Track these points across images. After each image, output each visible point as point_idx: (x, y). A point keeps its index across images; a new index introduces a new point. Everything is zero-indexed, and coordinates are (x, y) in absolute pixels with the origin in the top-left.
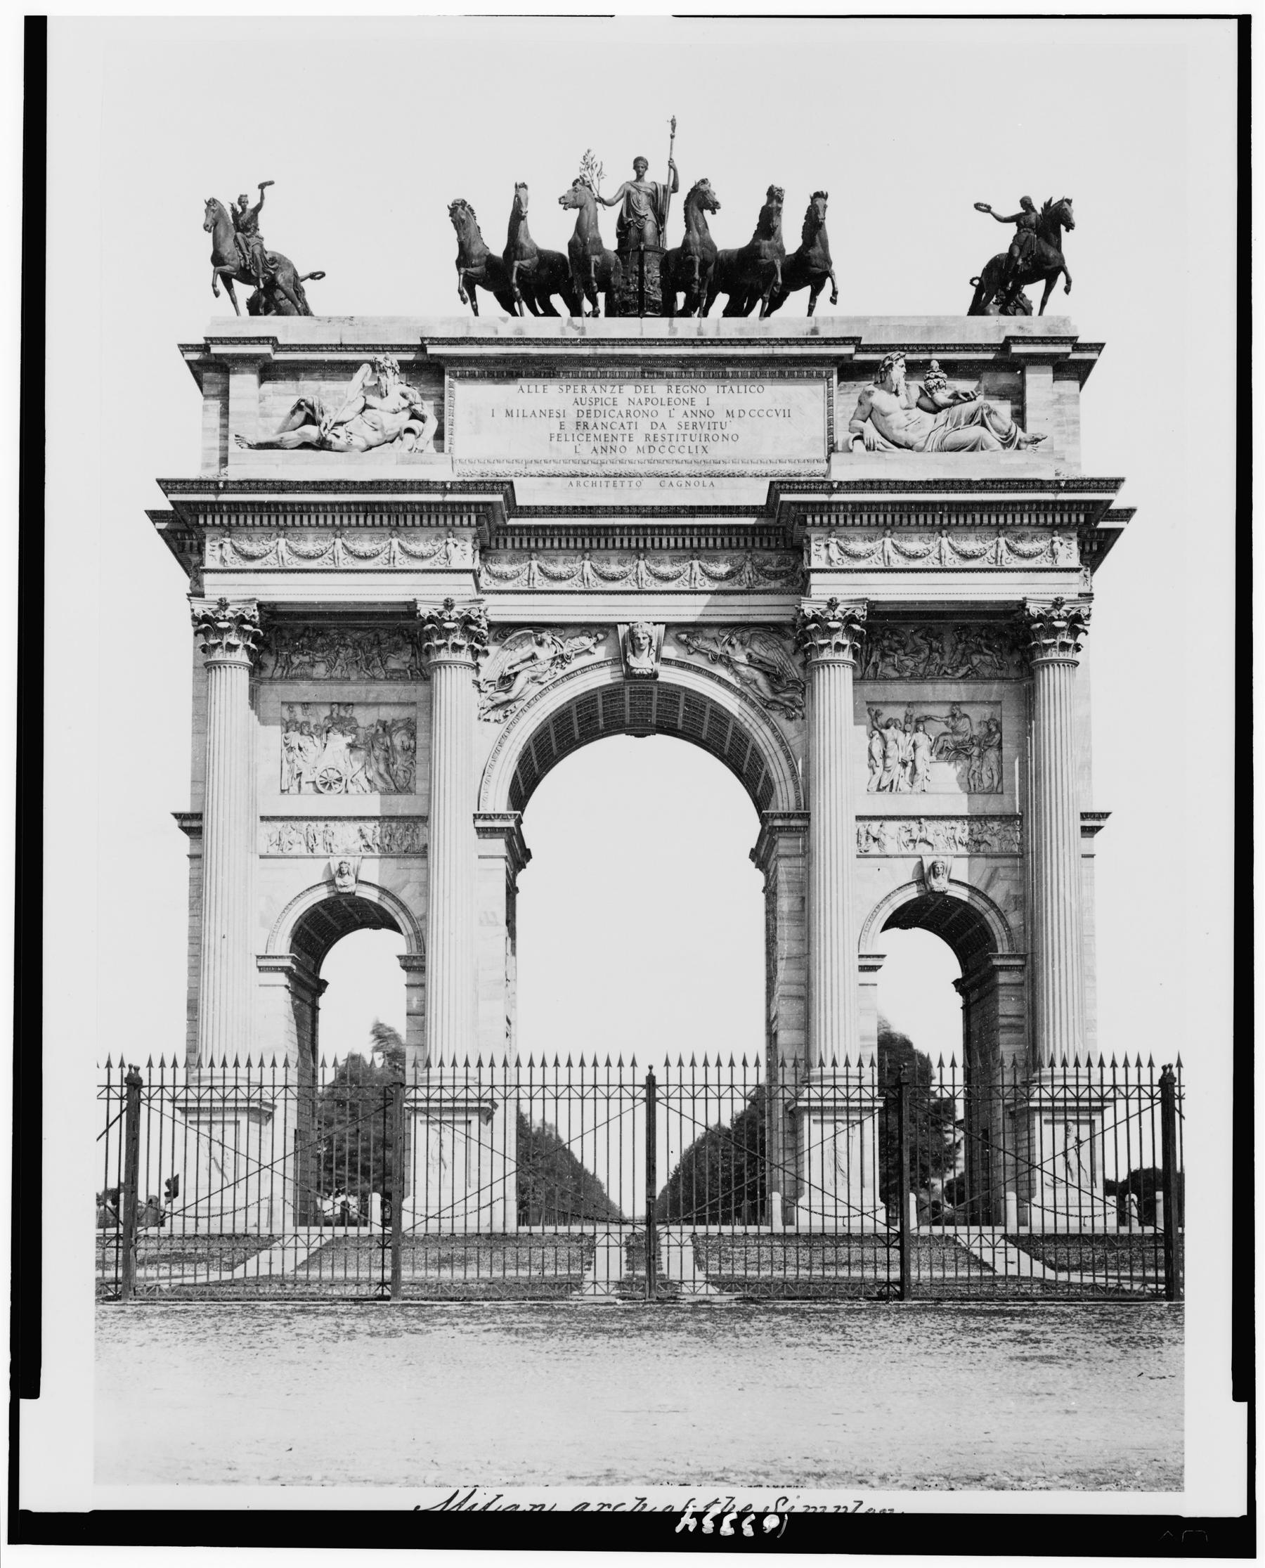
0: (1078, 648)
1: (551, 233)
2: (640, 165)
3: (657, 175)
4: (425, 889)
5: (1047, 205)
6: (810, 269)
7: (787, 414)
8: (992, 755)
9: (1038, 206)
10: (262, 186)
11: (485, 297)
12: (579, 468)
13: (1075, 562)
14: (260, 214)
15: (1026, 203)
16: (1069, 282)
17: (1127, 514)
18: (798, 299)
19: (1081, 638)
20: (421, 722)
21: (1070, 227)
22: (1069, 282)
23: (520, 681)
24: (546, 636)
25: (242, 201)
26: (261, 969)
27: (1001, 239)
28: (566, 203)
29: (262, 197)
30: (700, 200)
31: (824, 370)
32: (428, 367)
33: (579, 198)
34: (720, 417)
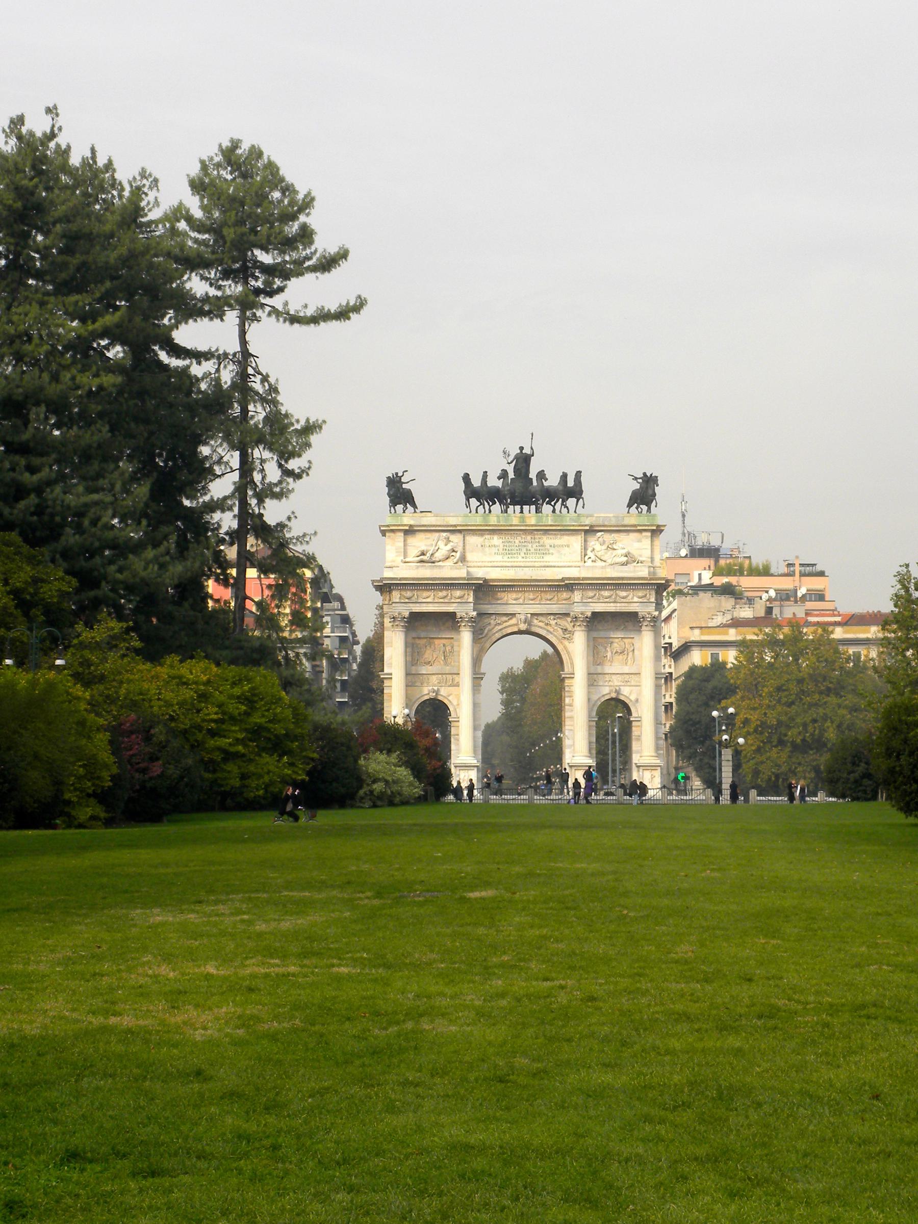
1: (494, 482)
2: (522, 448)
3: (527, 451)
4: (458, 697)
6: (576, 492)
7: (568, 546)
8: (631, 654)
9: (649, 475)
11: (474, 502)
12: (505, 564)
13: (653, 600)
15: (645, 474)
18: (571, 502)
20: (455, 644)
23: (486, 631)
24: (494, 616)
25: (397, 474)
28: (499, 478)
30: (541, 475)
33: (504, 475)
34: (548, 547)
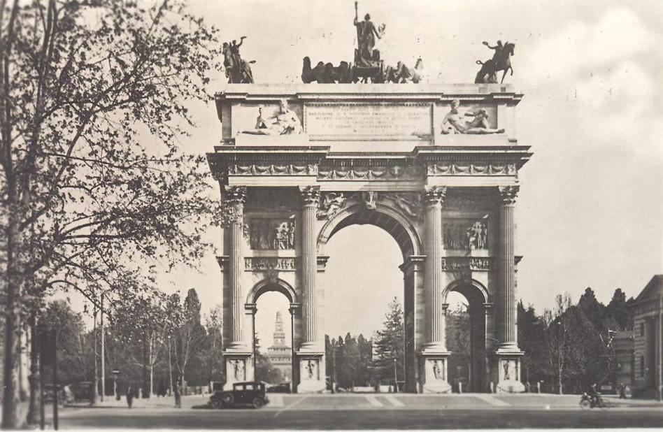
0: (515, 202)
5: (506, 44)
9: (503, 44)
10: (242, 38)
14: (240, 49)
15: (499, 43)
16: (512, 72)
17: (531, 154)
19: (515, 198)
21: (512, 54)
22: (512, 72)
25: (234, 42)
26: (246, 308)
27: (489, 55)
29: (241, 43)
31: (430, 103)
32: (298, 102)
